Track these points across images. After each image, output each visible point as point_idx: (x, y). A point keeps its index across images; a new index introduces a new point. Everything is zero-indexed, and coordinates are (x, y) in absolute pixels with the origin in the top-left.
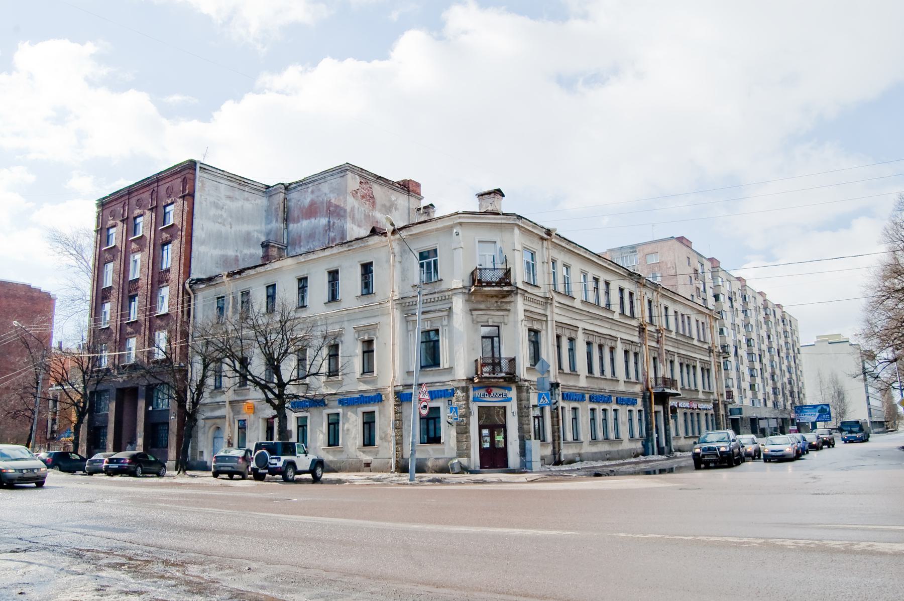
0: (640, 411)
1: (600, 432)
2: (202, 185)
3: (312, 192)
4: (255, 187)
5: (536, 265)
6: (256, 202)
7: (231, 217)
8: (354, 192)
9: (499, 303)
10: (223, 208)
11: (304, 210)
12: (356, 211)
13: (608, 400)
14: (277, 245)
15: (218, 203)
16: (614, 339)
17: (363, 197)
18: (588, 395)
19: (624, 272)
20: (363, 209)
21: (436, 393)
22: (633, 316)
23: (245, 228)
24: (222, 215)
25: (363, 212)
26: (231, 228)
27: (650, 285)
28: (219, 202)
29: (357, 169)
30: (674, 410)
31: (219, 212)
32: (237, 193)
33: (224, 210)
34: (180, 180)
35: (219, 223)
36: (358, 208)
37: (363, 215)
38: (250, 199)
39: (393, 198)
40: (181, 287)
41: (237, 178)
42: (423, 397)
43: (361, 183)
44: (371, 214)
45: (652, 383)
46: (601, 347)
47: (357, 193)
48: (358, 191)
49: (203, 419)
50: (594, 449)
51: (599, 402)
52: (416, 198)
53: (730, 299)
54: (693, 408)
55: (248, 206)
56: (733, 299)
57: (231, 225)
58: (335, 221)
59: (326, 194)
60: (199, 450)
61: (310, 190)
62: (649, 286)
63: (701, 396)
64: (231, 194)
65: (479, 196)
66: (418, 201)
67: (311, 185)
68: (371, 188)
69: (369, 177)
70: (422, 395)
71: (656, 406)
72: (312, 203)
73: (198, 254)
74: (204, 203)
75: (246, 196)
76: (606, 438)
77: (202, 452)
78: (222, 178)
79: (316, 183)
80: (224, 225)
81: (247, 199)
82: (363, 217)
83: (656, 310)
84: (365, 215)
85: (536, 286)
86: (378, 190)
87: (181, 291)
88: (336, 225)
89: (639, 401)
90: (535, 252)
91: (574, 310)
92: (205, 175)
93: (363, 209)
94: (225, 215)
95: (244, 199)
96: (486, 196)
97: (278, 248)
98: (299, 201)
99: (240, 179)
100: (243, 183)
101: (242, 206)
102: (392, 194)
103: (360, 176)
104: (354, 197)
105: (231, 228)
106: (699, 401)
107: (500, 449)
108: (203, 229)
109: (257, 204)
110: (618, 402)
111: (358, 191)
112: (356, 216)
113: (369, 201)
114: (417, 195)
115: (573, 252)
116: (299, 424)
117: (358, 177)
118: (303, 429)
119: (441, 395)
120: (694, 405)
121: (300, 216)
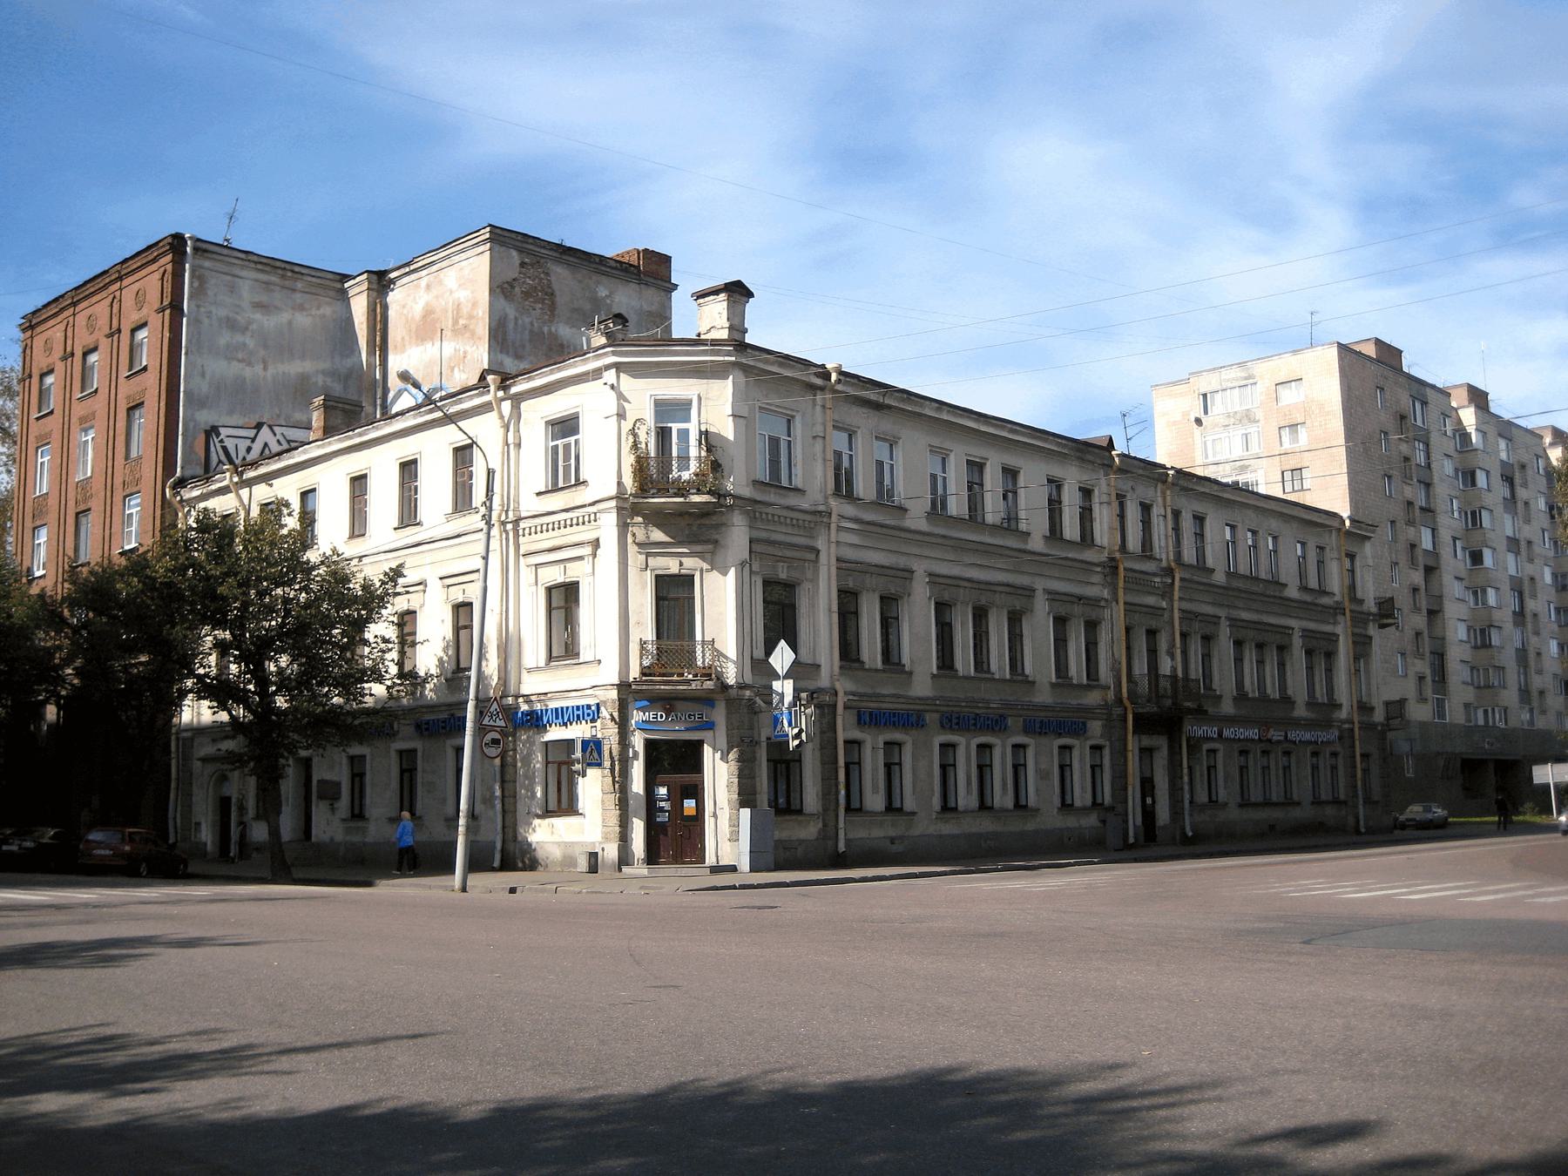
0: (1096, 748)
1: (875, 790)
2: (201, 285)
3: (428, 287)
4: (318, 281)
5: (795, 444)
6: (322, 311)
7: (265, 346)
8: (506, 286)
9: (695, 528)
10: (247, 328)
11: (414, 327)
12: (511, 326)
13: (996, 724)
14: (340, 405)
15: (235, 320)
16: (1029, 592)
17: (527, 295)
18: (936, 716)
19: (1059, 444)
20: (527, 320)
21: (570, 709)
22: (1087, 538)
23: (295, 368)
24: (244, 344)
25: (528, 326)
26: (265, 369)
27: (1143, 469)
28: (239, 318)
29: (514, 236)
30: (1194, 745)
31: (239, 338)
32: (278, 297)
33: (249, 334)
34: (157, 276)
35: (239, 361)
36: (516, 319)
37: (527, 332)
38: (307, 306)
39: (602, 292)
40: (159, 497)
41: (278, 264)
42: (492, 723)
43: (523, 264)
44: (546, 329)
45: (1144, 686)
46: (980, 615)
47: (513, 287)
48: (516, 284)
49: (199, 759)
50: (949, 828)
51: (968, 730)
52: (658, 287)
53: (1509, 480)
54: (1270, 741)
55: (303, 320)
56: (1517, 480)
57: (265, 362)
58: (468, 348)
59: (451, 292)
60: (194, 821)
61: (423, 283)
62: (1141, 472)
63: (1301, 711)
64: (264, 298)
65: (698, 298)
66: (663, 294)
67: (424, 272)
68: (547, 274)
69: (543, 251)
70: (487, 719)
71: (1089, 734)
72: (428, 313)
73: (194, 427)
74: (206, 321)
75: (298, 301)
76: (984, 806)
77: (198, 824)
78: (243, 267)
79: (434, 268)
80: (250, 364)
81: (301, 308)
82: (527, 335)
83: (1162, 523)
84: (531, 331)
85: (797, 490)
86: (561, 276)
87: (159, 503)
88: (469, 357)
89: (1095, 727)
90: (793, 417)
91: (903, 535)
92: (207, 264)
93: (527, 320)
94: (251, 343)
95: (293, 308)
96: (712, 297)
97: (344, 410)
98: (404, 307)
99: (283, 265)
100: (289, 274)
101: (290, 323)
102: (598, 283)
103: (520, 251)
104: (506, 297)
105: (265, 369)
106: (1297, 723)
107: (690, 818)
108: (203, 375)
109: (324, 316)
110: (1028, 729)
111: (516, 284)
112: (511, 336)
113: (542, 301)
114: (660, 282)
115: (903, 410)
116: (404, 766)
117: (514, 253)
118: (411, 776)
119: (578, 716)
120: (1275, 735)
121: (407, 338)
